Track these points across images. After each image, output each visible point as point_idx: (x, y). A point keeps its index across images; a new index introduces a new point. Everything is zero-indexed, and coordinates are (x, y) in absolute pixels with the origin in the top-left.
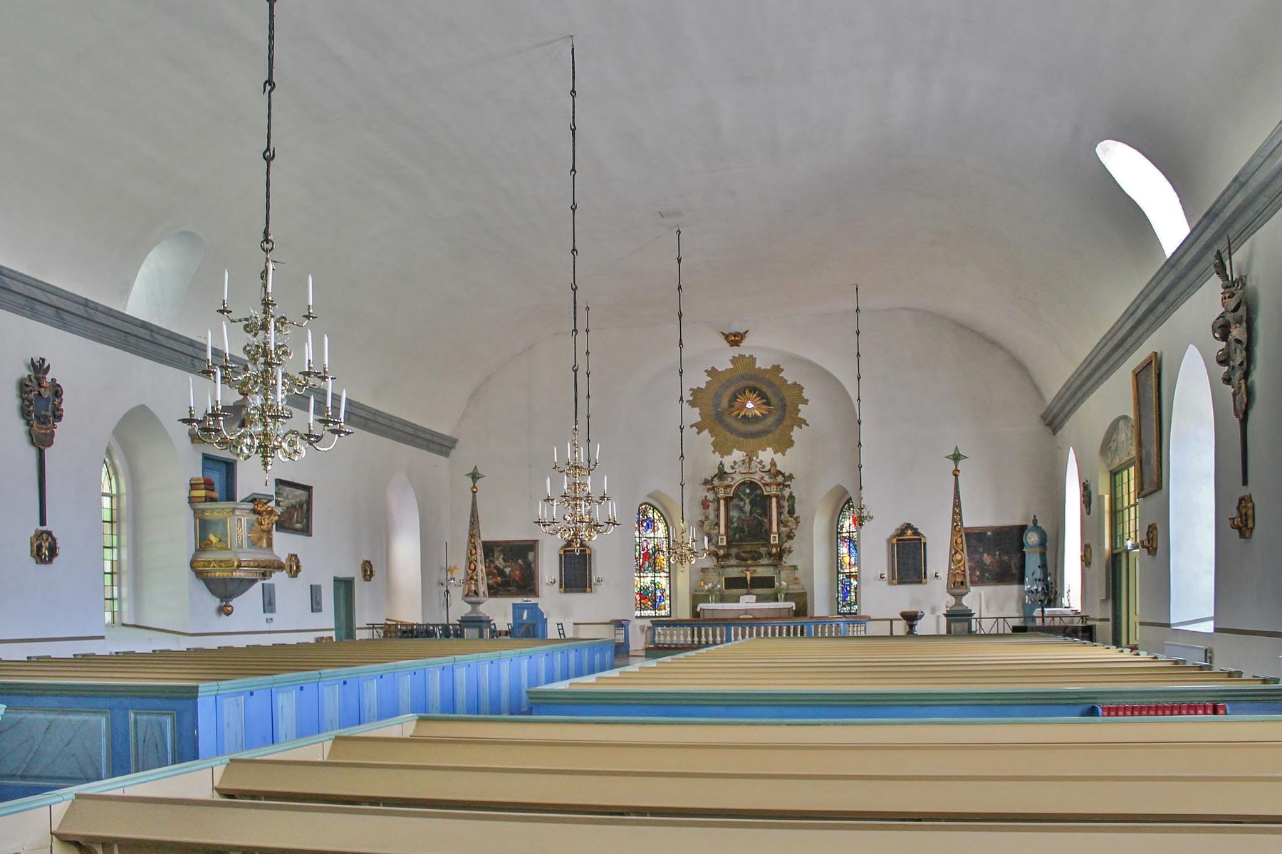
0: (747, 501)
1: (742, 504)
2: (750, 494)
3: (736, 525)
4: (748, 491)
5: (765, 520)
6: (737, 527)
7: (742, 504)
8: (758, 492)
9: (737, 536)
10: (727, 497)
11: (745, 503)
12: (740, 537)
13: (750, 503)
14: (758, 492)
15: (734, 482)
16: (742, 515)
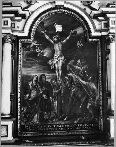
0: (58, 47)
1: (46, 53)
2: (62, 35)
3: (33, 93)
4: (59, 28)
5: (93, 86)
6: (36, 99)
7: (46, 53)
8: (79, 31)
9: (36, 117)
10: (18, 38)
11: (53, 52)
12: (41, 119)
13: (63, 52)
14: (79, 31)
15: (31, 9)
16: (48, 75)
